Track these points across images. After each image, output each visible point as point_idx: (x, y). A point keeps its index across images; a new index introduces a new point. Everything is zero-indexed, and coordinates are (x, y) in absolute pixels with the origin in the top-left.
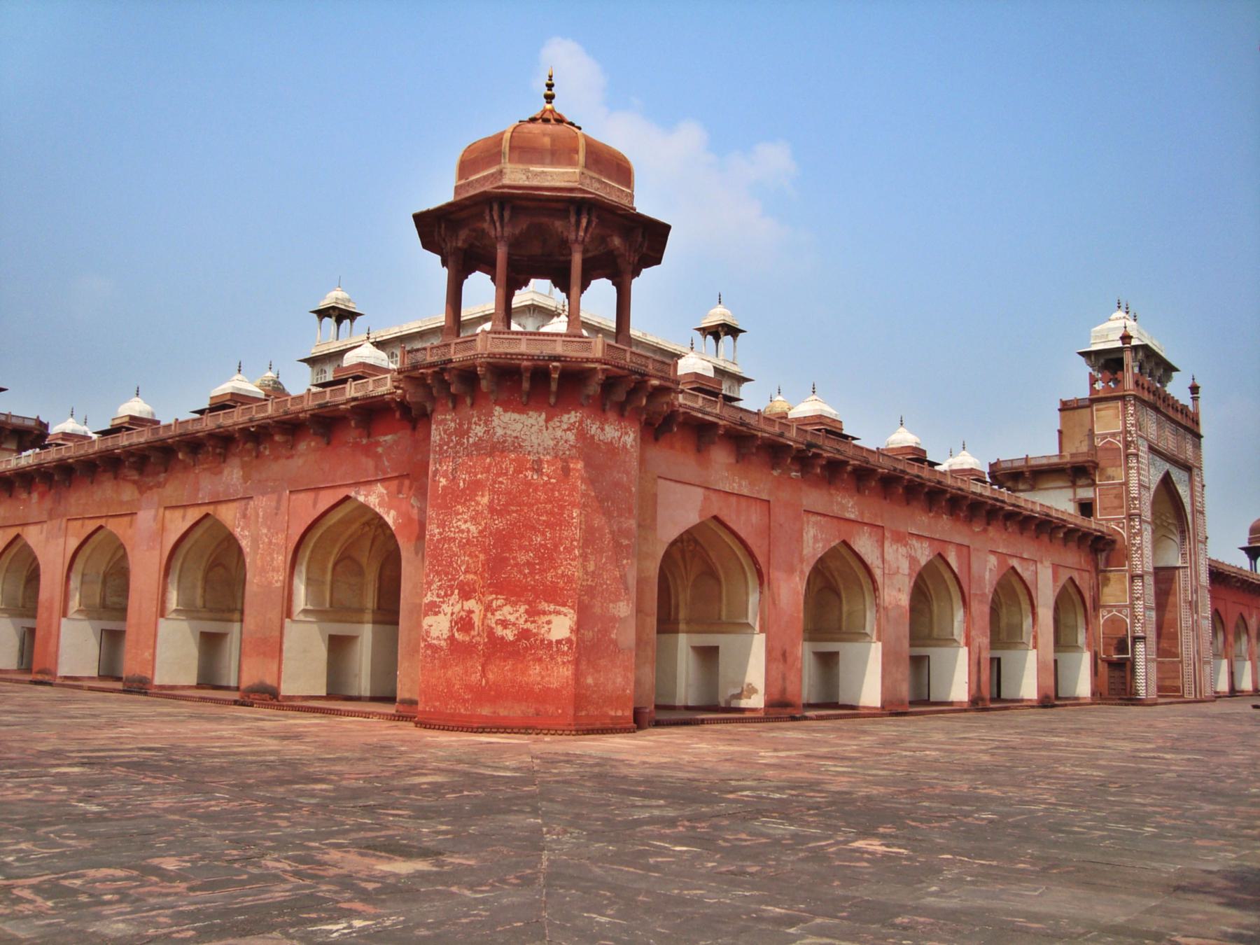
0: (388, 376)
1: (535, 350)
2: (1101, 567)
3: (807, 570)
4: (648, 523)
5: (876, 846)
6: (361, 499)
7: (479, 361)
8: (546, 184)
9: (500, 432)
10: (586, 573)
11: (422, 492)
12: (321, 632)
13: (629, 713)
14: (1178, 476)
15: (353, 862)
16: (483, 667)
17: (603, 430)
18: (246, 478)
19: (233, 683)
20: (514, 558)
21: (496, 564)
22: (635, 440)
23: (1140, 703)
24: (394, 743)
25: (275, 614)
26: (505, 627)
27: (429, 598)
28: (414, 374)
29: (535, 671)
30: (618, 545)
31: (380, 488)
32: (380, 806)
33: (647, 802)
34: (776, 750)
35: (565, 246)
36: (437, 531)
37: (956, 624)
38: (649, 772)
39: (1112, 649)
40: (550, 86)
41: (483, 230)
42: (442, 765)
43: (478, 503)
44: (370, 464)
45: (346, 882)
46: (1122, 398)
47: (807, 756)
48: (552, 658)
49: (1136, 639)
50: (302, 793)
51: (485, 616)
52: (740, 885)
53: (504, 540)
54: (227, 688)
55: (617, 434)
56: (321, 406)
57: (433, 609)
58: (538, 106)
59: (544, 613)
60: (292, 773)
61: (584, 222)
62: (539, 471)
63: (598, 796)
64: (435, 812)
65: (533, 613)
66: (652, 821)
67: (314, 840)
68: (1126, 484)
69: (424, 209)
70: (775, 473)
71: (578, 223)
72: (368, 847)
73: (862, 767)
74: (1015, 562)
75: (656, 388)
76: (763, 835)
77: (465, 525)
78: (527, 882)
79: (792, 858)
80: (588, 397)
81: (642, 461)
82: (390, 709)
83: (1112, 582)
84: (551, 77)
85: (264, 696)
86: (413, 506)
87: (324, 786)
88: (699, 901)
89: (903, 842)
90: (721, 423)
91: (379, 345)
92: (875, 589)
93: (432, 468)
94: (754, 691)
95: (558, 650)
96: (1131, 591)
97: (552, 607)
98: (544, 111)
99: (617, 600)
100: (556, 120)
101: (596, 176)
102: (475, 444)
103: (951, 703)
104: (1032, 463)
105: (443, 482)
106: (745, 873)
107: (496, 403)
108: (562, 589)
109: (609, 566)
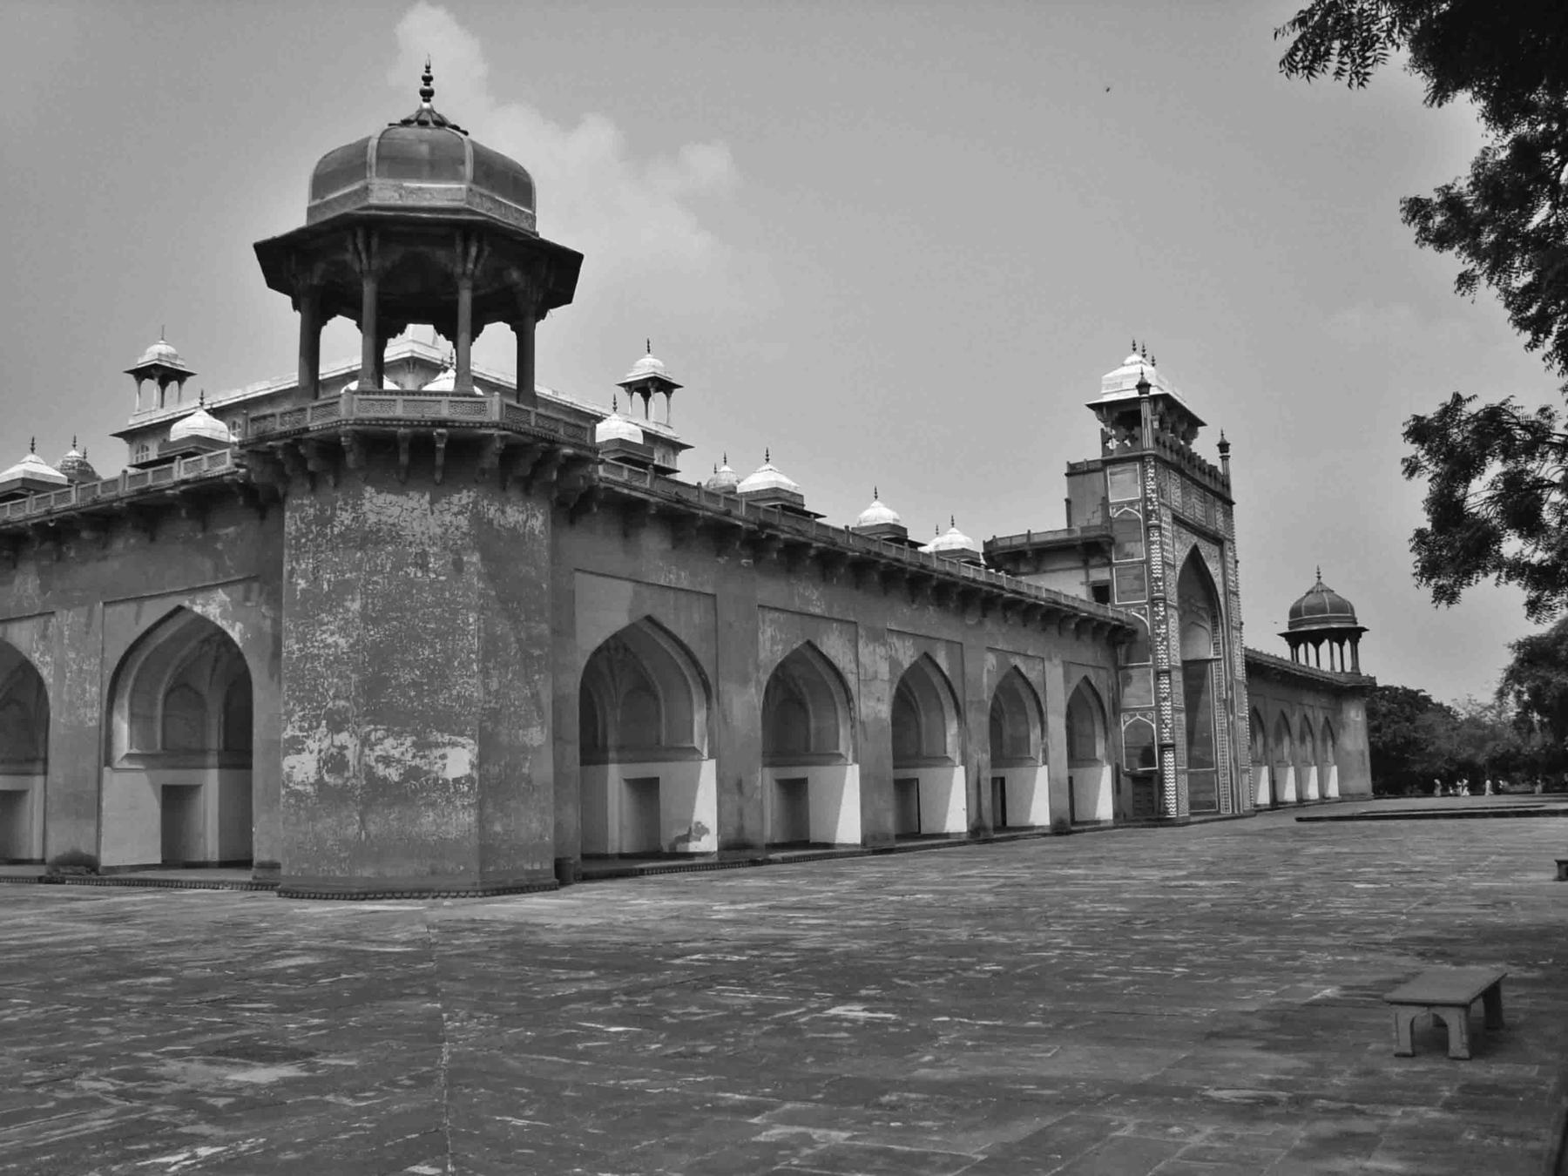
0: (228, 451)
1: (414, 415)
2: (1122, 663)
3: (765, 678)
4: (564, 630)
5: (856, 1012)
6: (198, 609)
7: (343, 429)
8: (425, 204)
9: (372, 518)
10: (489, 693)
11: (274, 599)
12: (153, 783)
13: (549, 866)
14: (1207, 550)
15: (198, 1073)
16: (361, 815)
17: (503, 512)
18: (44, 588)
19: (37, 855)
20: (397, 678)
21: (373, 687)
22: (544, 524)
23: (1171, 823)
24: (250, 919)
25: (90, 762)
26: (388, 765)
27: (289, 732)
28: (261, 448)
29: (428, 819)
30: (527, 659)
31: (221, 595)
32: (234, 999)
33: (573, 975)
34: (733, 903)
35: (449, 283)
36: (296, 647)
37: (949, 740)
38: (577, 937)
39: (1136, 762)
40: (427, 80)
41: (345, 262)
42: (314, 943)
43: (347, 610)
44: (208, 565)
45: (190, 1100)
46: (1141, 459)
47: (771, 908)
48: (449, 801)
49: (1164, 748)
50: (130, 991)
51: (362, 752)
52: (692, 1069)
53: (380, 656)
54: (30, 862)
55: (521, 517)
56: (141, 492)
57: (296, 746)
58: (412, 105)
59: (437, 745)
60: (117, 964)
61: (473, 251)
62: (424, 567)
63: (512, 970)
64: (303, 1002)
65: (422, 746)
66: (582, 997)
67: (145, 1049)
68: (1148, 561)
69: (268, 236)
70: (721, 561)
71: (466, 253)
72: (218, 1053)
73: (838, 917)
74: (1017, 661)
75: (568, 458)
76: (717, 1006)
77: (332, 638)
78: (423, 1081)
79: (754, 1032)
80: (483, 472)
81: (555, 550)
82: (245, 876)
83: (1135, 679)
84: (428, 68)
85: (79, 869)
86: (264, 616)
87: (159, 979)
88: (640, 1092)
89: (891, 1005)
90: (652, 499)
91: (217, 413)
92: (849, 699)
93: (287, 568)
94: (705, 831)
95: (456, 791)
96: (1157, 690)
97: (447, 738)
98: (421, 111)
99: (528, 725)
100: (436, 123)
101: (486, 192)
102: (341, 534)
103: (947, 835)
104: (1036, 539)
105: (302, 584)
106: (695, 1054)
107: (367, 481)
108: (458, 715)
109: (517, 683)
